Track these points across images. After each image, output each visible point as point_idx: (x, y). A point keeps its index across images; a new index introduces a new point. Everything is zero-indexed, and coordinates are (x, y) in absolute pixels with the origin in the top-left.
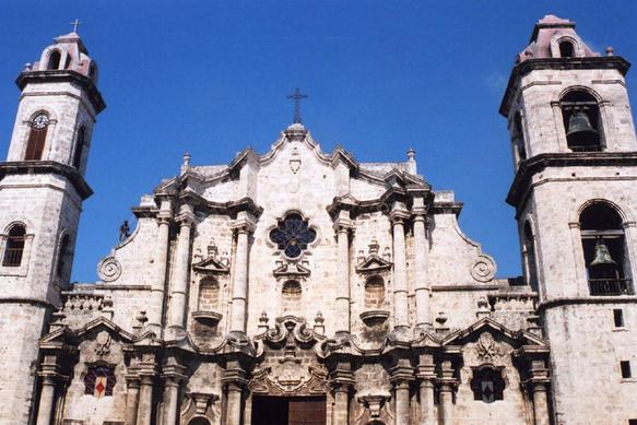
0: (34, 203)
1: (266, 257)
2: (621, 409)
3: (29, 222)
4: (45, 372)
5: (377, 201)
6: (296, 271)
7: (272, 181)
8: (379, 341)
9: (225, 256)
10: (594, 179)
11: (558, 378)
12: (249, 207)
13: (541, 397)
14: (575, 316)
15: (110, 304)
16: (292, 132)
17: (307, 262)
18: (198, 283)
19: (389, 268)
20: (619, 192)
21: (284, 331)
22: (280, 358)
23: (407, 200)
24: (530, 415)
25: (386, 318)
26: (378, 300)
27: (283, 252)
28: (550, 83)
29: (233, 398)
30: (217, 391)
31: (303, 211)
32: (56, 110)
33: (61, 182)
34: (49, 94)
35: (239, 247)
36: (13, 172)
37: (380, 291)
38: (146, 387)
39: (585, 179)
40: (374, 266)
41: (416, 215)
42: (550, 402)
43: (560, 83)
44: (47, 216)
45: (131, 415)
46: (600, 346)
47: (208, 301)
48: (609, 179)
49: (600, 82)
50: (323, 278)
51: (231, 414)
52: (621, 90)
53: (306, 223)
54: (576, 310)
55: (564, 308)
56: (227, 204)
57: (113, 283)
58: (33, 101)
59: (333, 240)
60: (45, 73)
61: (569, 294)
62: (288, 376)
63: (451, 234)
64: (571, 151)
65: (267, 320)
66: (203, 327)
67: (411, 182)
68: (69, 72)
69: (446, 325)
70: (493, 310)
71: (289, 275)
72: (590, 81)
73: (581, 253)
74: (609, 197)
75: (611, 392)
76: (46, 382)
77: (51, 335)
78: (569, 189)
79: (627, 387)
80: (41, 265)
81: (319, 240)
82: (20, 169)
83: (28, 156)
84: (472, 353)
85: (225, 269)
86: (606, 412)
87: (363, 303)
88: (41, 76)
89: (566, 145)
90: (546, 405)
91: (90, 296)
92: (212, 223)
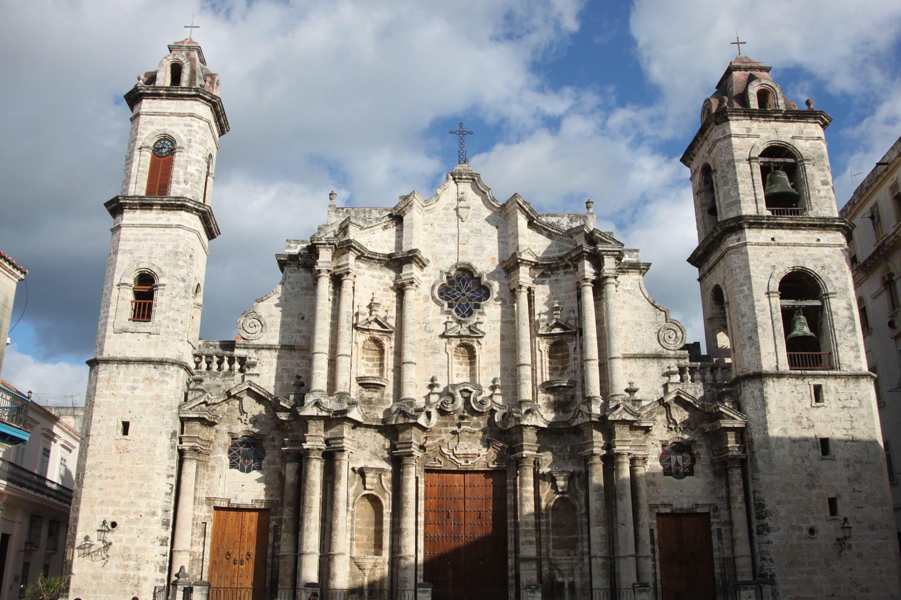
0: (162, 246)
2: (820, 487)
3: (160, 269)
4: (186, 445)
5: (561, 258)
6: (468, 333)
7: (438, 230)
8: (566, 412)
9: (390, 314)
10: (795, 245)
11: (756, 454)
13: (736, 474)
14: (775, 391)
15: (253, 365)
16: (460, 174)
18: (360, 345)
19: (575, 334)
20: (819, 260)
21: (459, 396)
22: (455, 428)
23: (597, 261)
24: (723, 493)
25: (572, 387)
26: (560, 367)
27: (453, 310)
28: (748, 136)
29: (408, 473)
30: (388, 467)
31: (474, 264)
32: (182, 136)
33: (193, 222)
34: (171, 114)
36: (132, 207)
37: (563, 357)
39: (786, 245)
40: (557, 330)
41: (607, 277)
42: (744, 476)
43: (758, 137)
44: (181, 263)
45: (289, 493)
46: (800, 423)
47: (371, 364)
48: (809, 245)
49: (800, 138)
51: (407, 491)
52: (823, 147)
53: (479, 278)
54: (776, 384)
55: (762, 383)
56: (390, 256)
58: (152, 123)
59: (508, 302)
60: (167, 89)
61: (768, 365)
63: (638, 297)
64: (769, 213)
65: (438, 386)
66: (367, 394)
67: (602, 241)
68: (197, 90)
69: (637, 396)
70: (682, 380)
71: (460, 336)
72: (791, 136)
73: (780, 325)
74: (810, 266)
75: (811, 469)
76: (187, 456)
77: (192, 401)
78: (768, 256)
79: (825, 465)
80: (175, 320)
82: (145, 206)
83: (150, 191)
84: (661, 426)
86: (806, 490)
88: (161, 92)
89: (764, 206)
90: (741, 483)
92: (373, 277)
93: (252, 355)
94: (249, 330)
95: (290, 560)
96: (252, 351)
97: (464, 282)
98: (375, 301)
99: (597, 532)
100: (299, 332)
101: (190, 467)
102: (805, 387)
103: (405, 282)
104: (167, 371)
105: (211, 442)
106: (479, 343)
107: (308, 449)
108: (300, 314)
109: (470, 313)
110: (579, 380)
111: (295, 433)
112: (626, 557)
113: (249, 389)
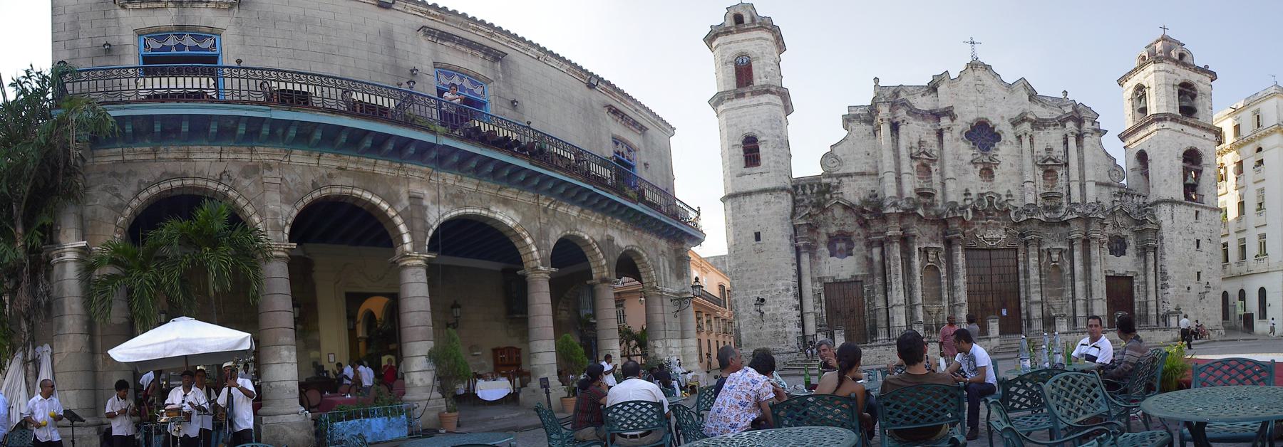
1: (967, 151)
12: (949, 113)
17: (997, 155)
25: (1060, 197)
27: (977, 147)
35: (946, 143)
37: (1052, 180)
38: (896, 244)
50: (1009, 167)
56: (931, 111)
57: (837, 172)
62: (996, 235)
81: (1005, 141)
85: (936, 158)
87: (1042, 187)
91: (820, 184)
93: (834, 181)
94: (832, 165)
95: (884, 311)
96: (835, 179)
97: (982, 129)
98: (922, 140)
99: (1079, 285)
100: (867, 163)
101: (805, 258)
102: (1192, 211)
103: (943, 127)
104: (780, 195)
105: (815, 241)
106: (996, 168)
107: (890, 236)
108: (866, 151)
109: (988, 149)
110: (1065, 194)
111: (876, 228)
112: (1098, 299)
113: (837, 203)
